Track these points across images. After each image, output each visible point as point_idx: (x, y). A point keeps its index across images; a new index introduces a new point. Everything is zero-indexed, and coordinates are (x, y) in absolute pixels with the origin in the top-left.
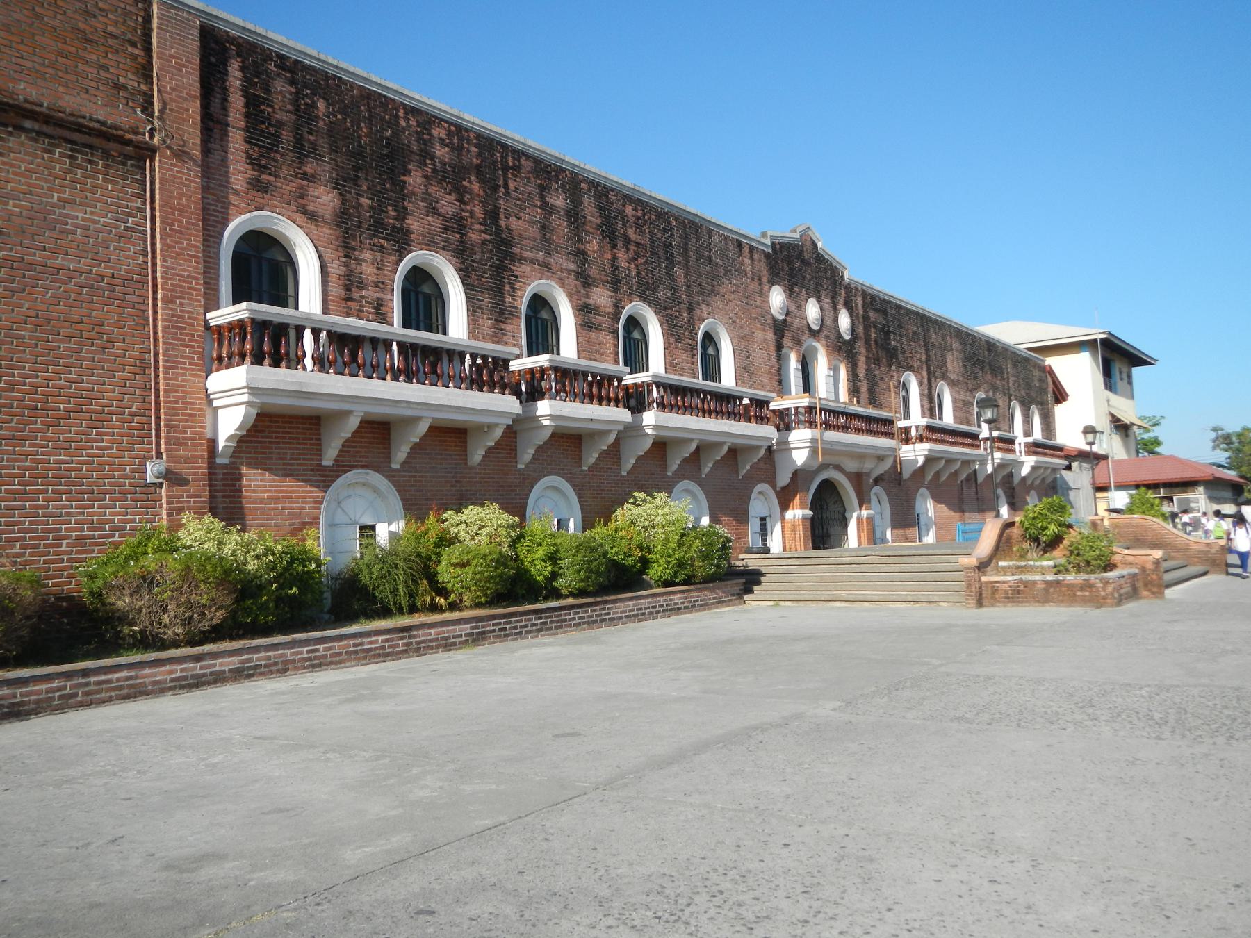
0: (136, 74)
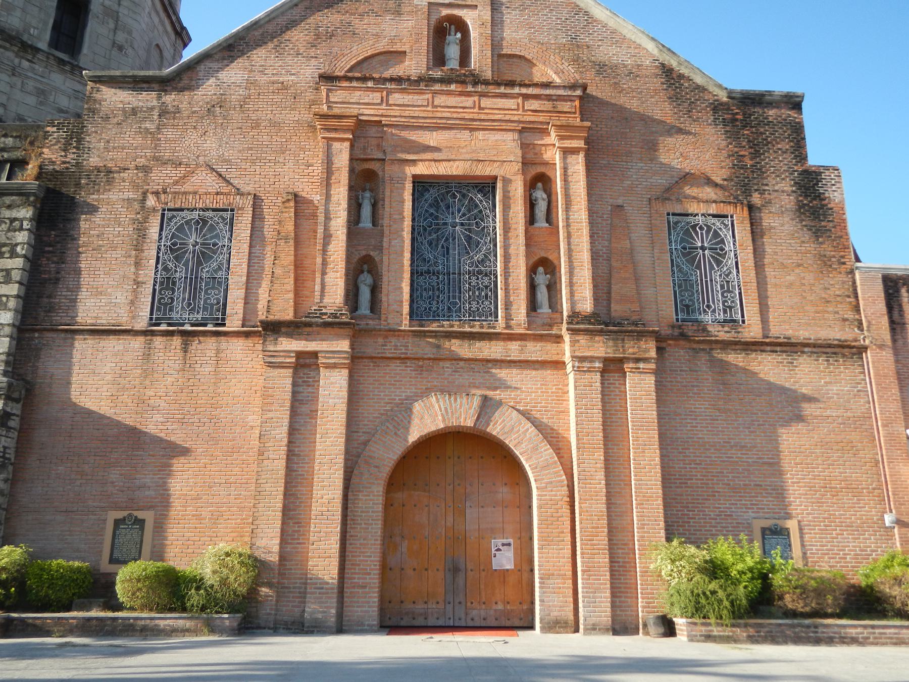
0: (852, 311)
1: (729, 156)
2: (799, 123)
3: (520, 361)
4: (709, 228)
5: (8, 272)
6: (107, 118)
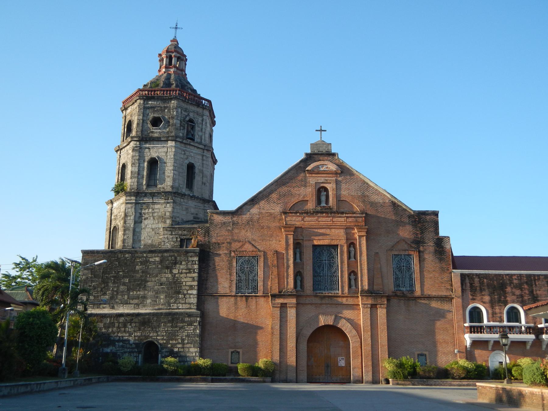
1: (413, 234)
2: (437, 221)
3: (346, 304)
4: (406, 259)
5: (193, 278)
6: (216, 226)
